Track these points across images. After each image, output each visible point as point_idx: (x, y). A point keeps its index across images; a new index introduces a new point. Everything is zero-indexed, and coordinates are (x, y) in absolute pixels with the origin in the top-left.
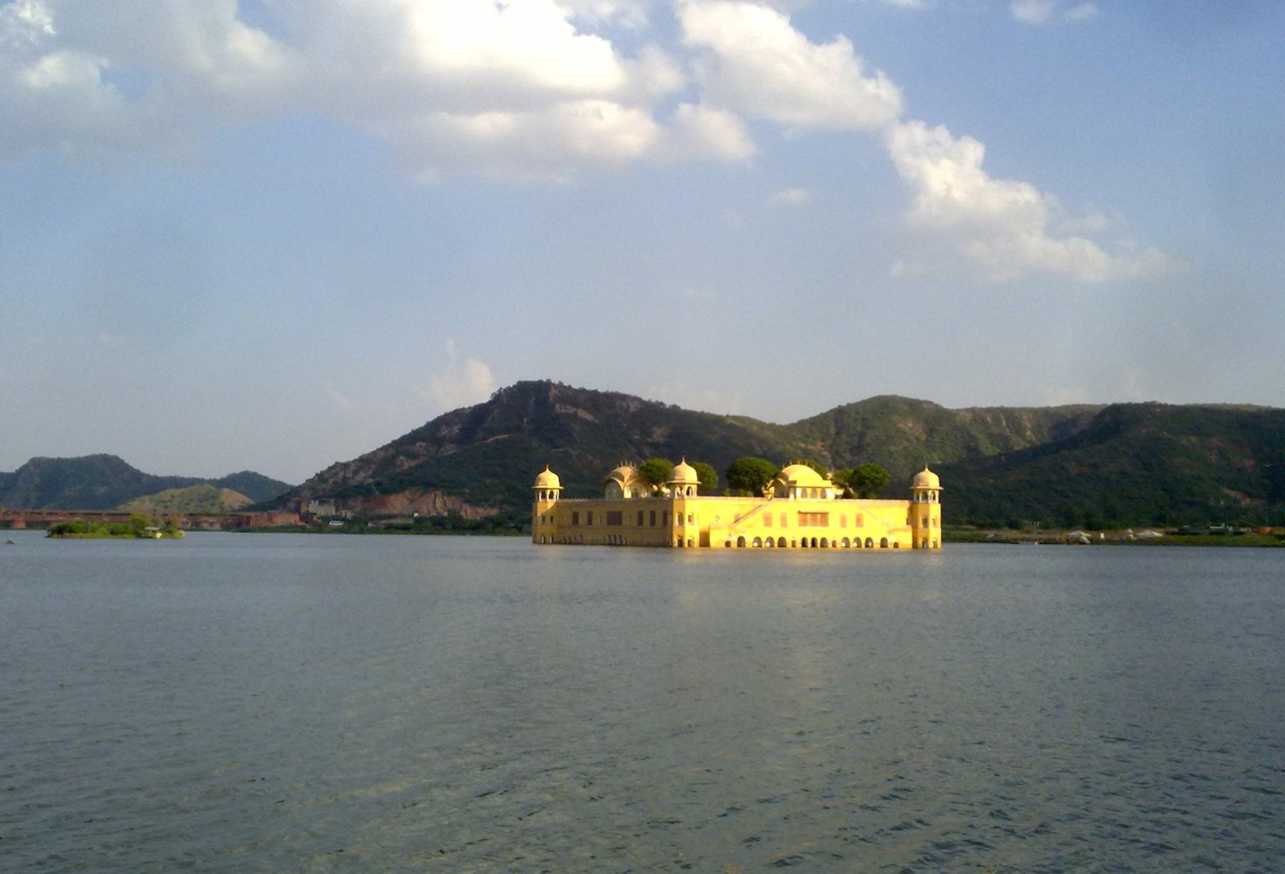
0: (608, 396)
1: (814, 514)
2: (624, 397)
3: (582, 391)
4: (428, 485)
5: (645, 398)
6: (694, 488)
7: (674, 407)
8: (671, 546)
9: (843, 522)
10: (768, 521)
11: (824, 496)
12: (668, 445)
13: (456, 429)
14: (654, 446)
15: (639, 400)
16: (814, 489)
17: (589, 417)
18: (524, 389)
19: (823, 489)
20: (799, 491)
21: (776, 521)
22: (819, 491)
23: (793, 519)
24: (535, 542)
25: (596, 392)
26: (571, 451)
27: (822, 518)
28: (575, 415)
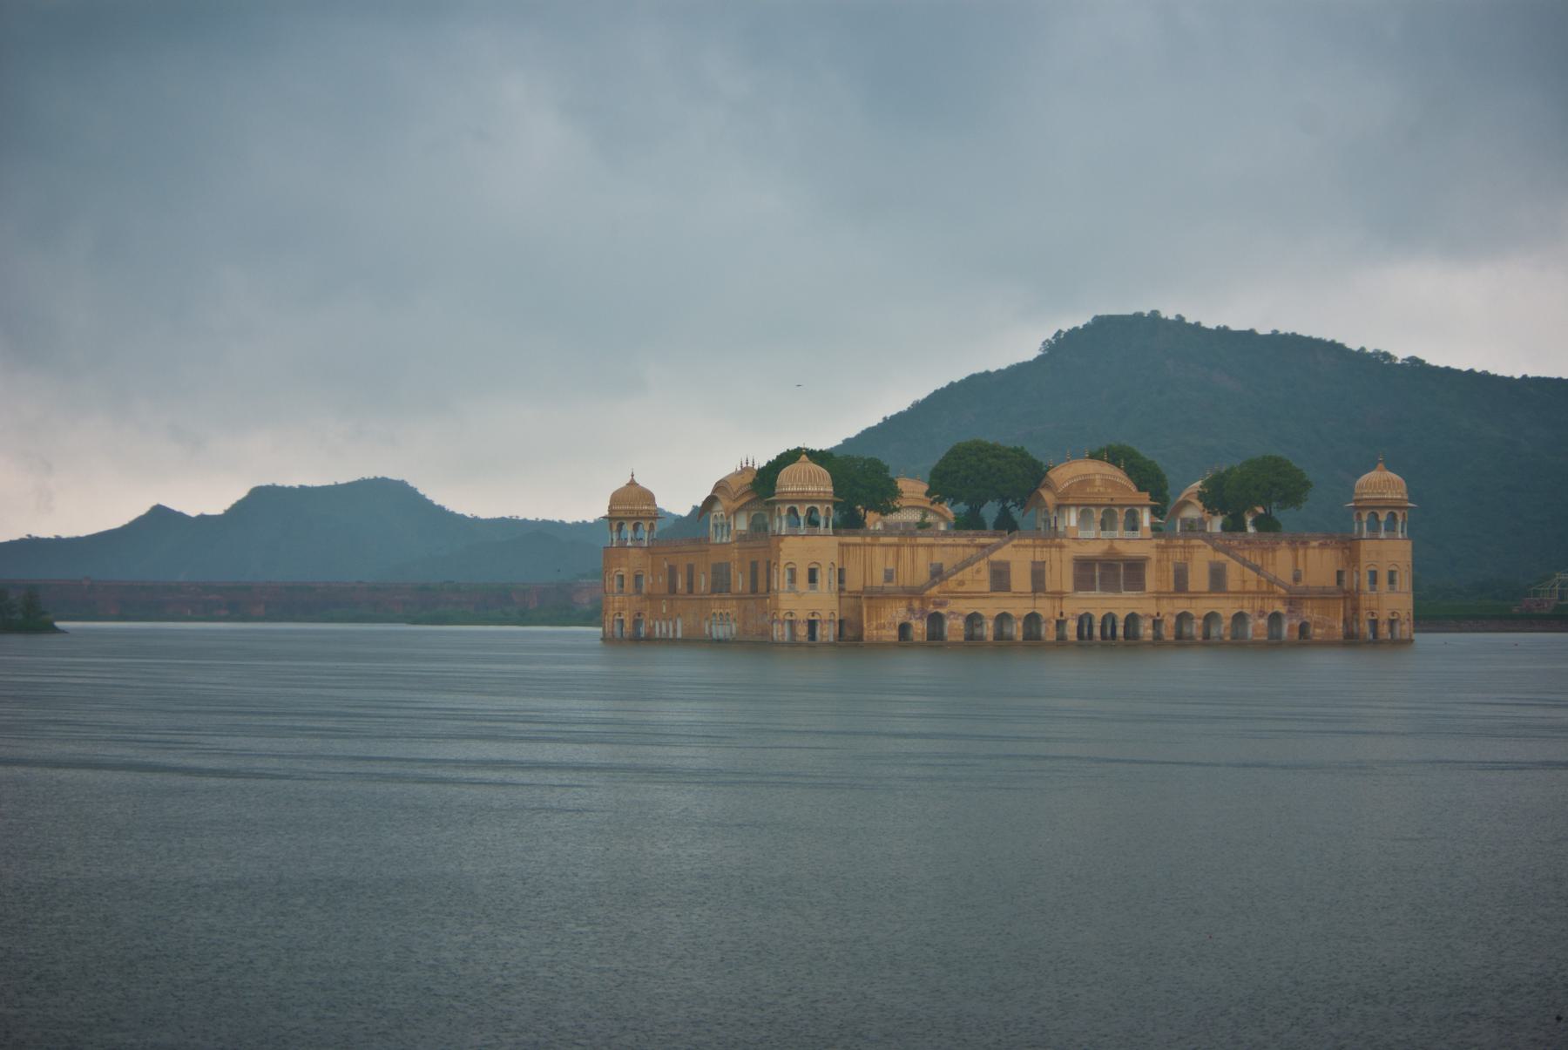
10: (1000, 579)
11: (1133, 524)
21: (1021, 579)
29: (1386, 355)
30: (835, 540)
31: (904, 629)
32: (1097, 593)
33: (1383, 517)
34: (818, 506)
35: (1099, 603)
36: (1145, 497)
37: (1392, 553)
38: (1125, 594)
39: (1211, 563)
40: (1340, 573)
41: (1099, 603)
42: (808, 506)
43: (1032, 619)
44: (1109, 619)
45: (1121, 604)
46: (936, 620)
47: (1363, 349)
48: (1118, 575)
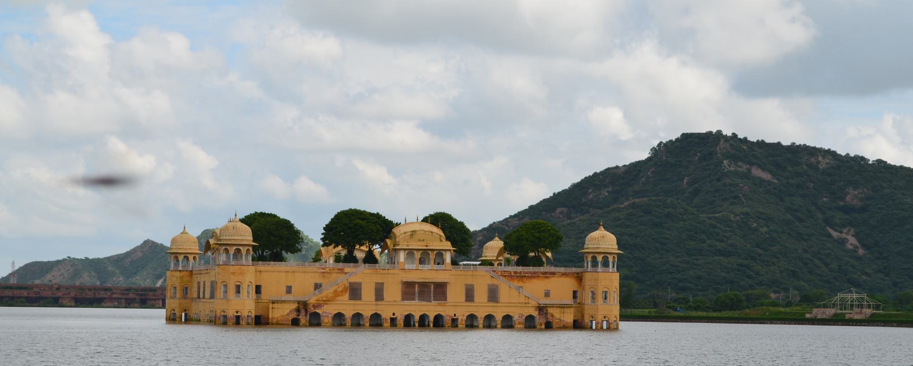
1: (424, 286)
3: (761, 144)
5: (842, 152)
6: (251, 249)
7: (880, 161)
8: (345, 325)
9: (470, 296)
13: (605, 193)
14: (847, 210)
16: (425, 252)
17: (766, 176)
19: (440, 254)
21: (368, 293)
22: (432, 256)
23: (393, 292)
24: (172, 319)
25: (779, 144)
26: (732, 217)
28: (747, 176)
29: (863, 158)
30: (252, 269)
32: (416, 302)
33: (600, 258)
34: (241, 248)
35: (417, 308)
36: (448, 245)
37: (609, 280)
38: (434, 303)
39: (489, 285)
40: (575, 293)
41: (417, 308)
42: (235, 248)
44: (423, 318)
45: (432, 309)
47: (848, 154)
48: (430, 291)
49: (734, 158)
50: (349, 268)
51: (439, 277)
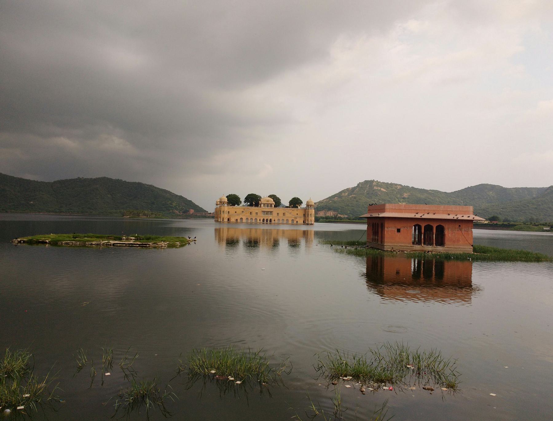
0: (391, 184)
2: (396, 185)
3: (383, 183)
4: (330, 209)
11: (271, 206)
12: (408, 198)
13: (346, 194)
14: (404, 198)
15: (401, 185)
17: (385, 190)
18: (366, 182)
20: (262, 205)
27: (271, 212)
28: (380, 190)
31: (237, 220)
43: (256, 219)
44: (267, 220)
45: (269, 217)
46: (241, 219)
49: (377, 186)
50: (250, 207)
51: (271, 210)
